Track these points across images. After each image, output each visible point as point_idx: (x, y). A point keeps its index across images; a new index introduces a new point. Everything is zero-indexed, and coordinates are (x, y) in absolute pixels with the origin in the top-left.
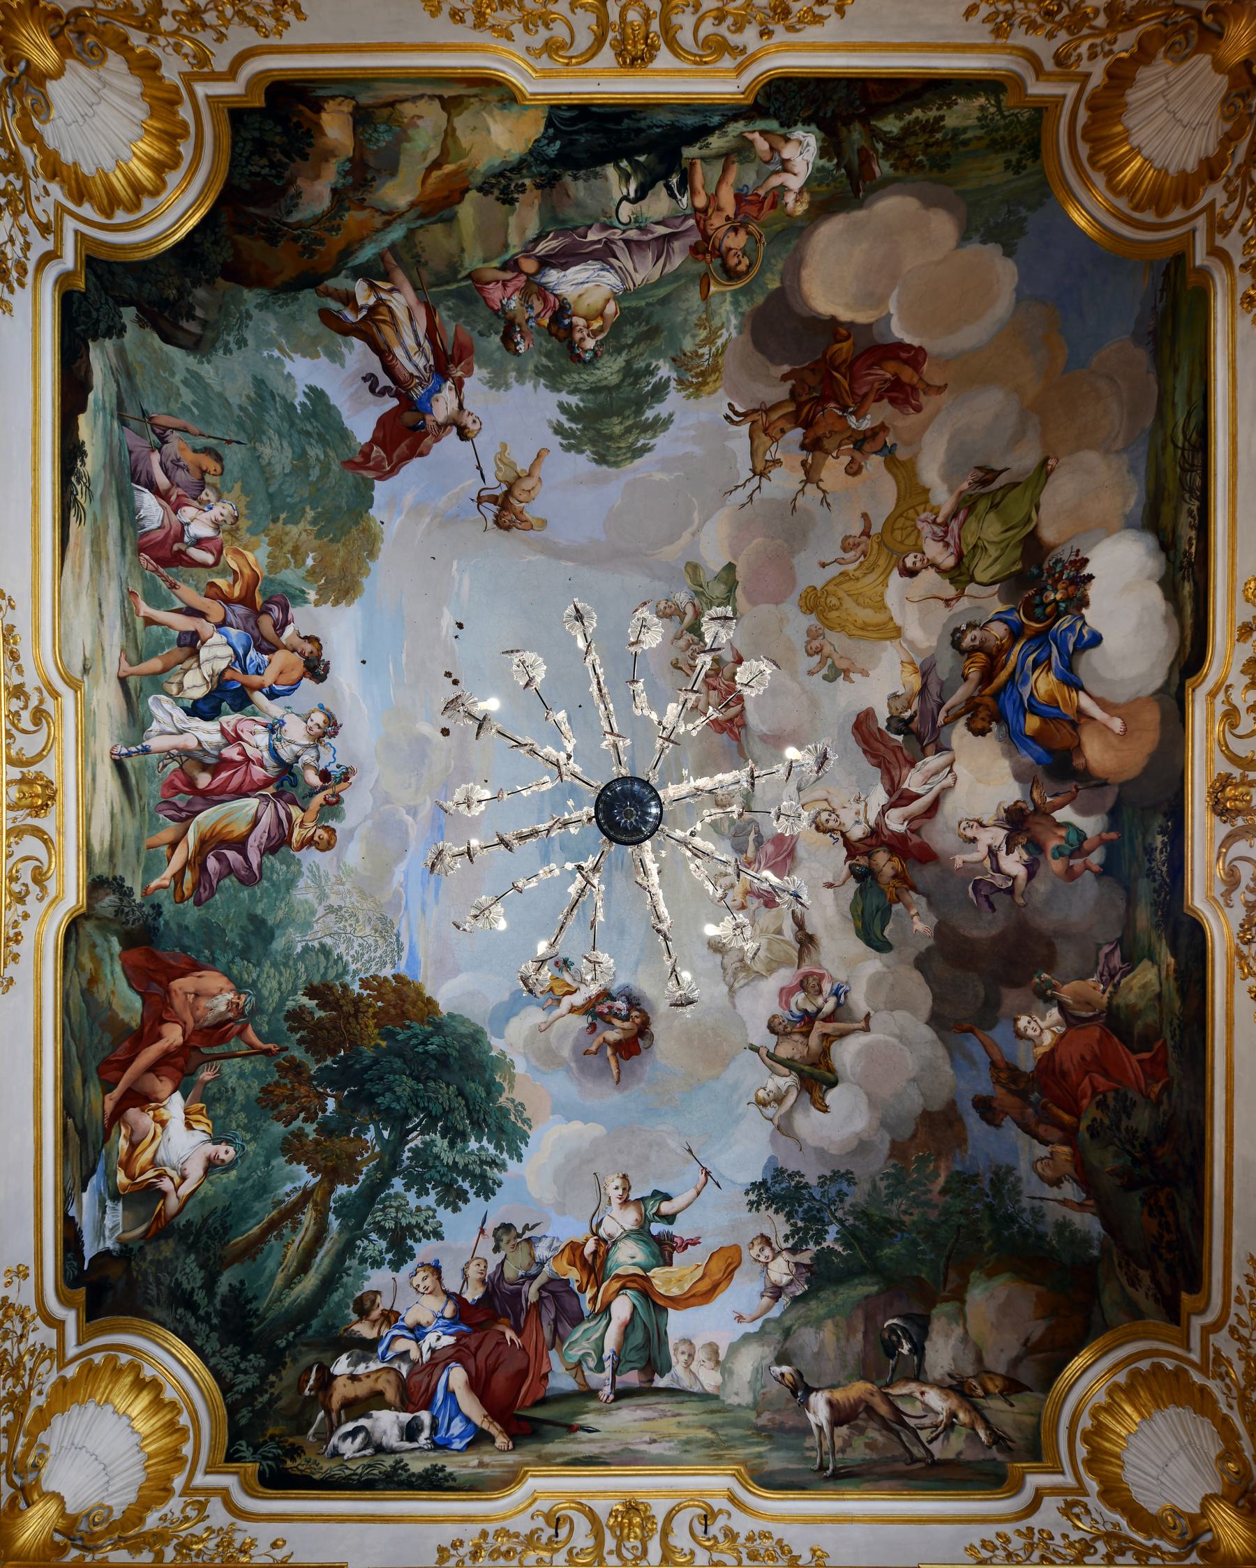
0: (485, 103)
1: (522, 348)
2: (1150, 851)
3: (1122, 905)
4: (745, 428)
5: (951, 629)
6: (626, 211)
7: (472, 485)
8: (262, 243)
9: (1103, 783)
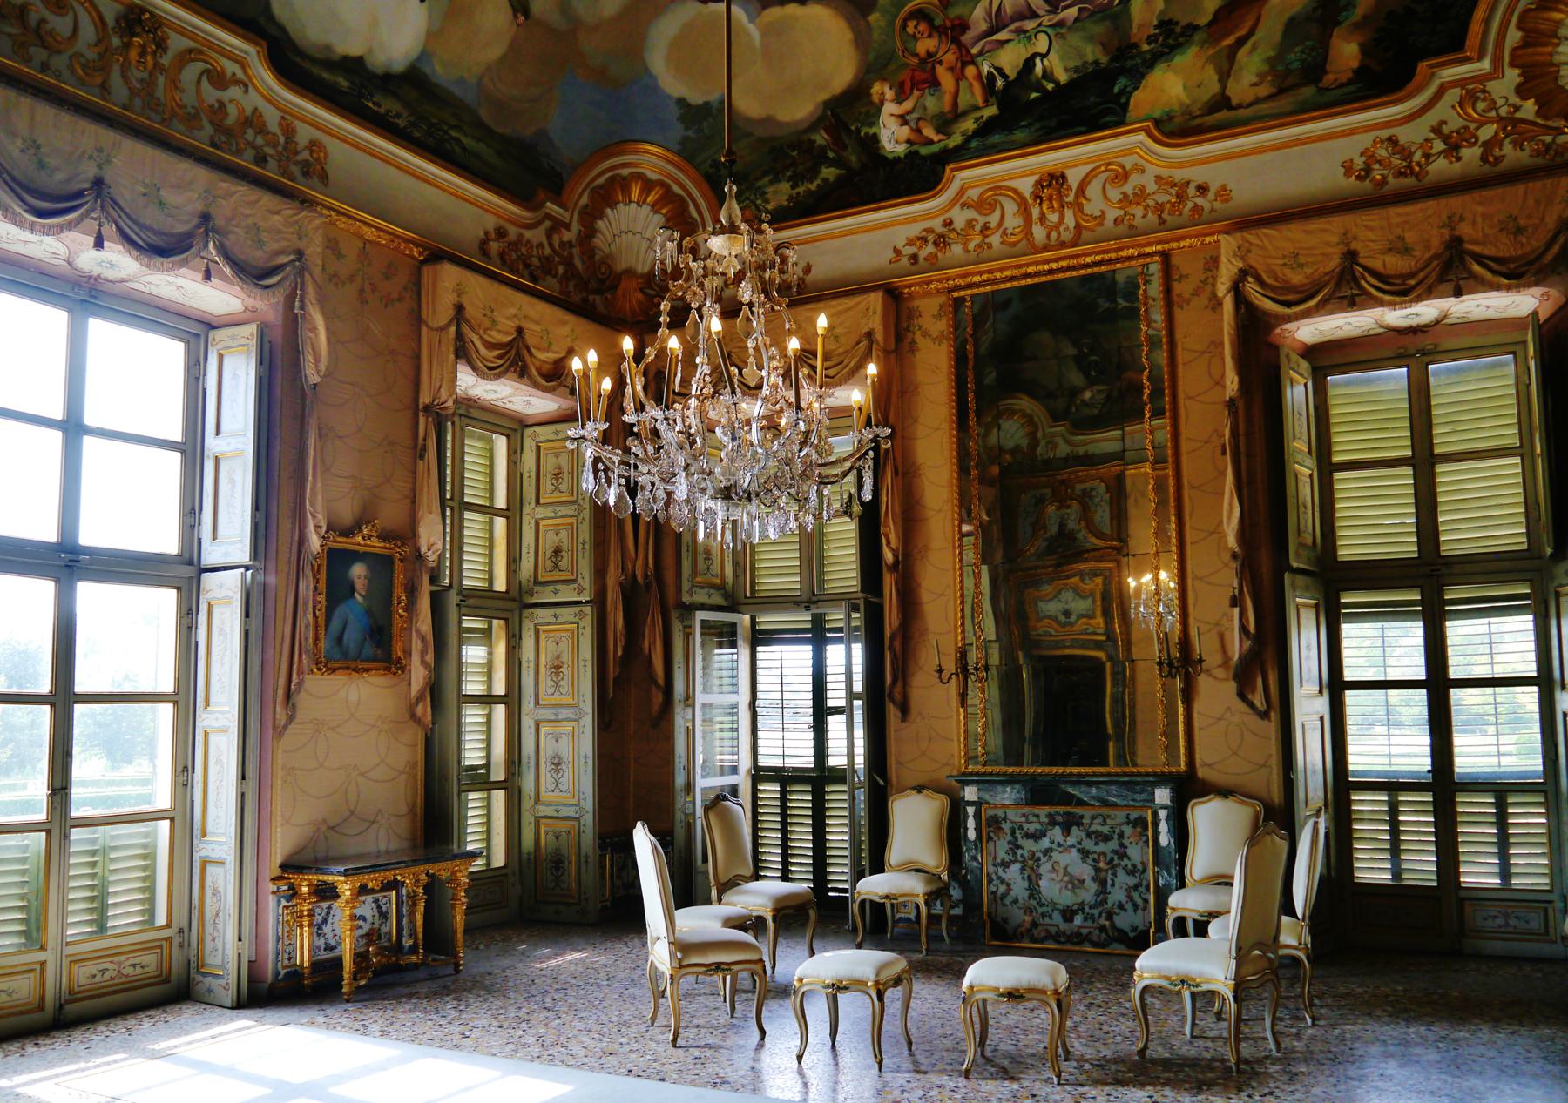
0: (1187, 112)
6: (1042, 44)
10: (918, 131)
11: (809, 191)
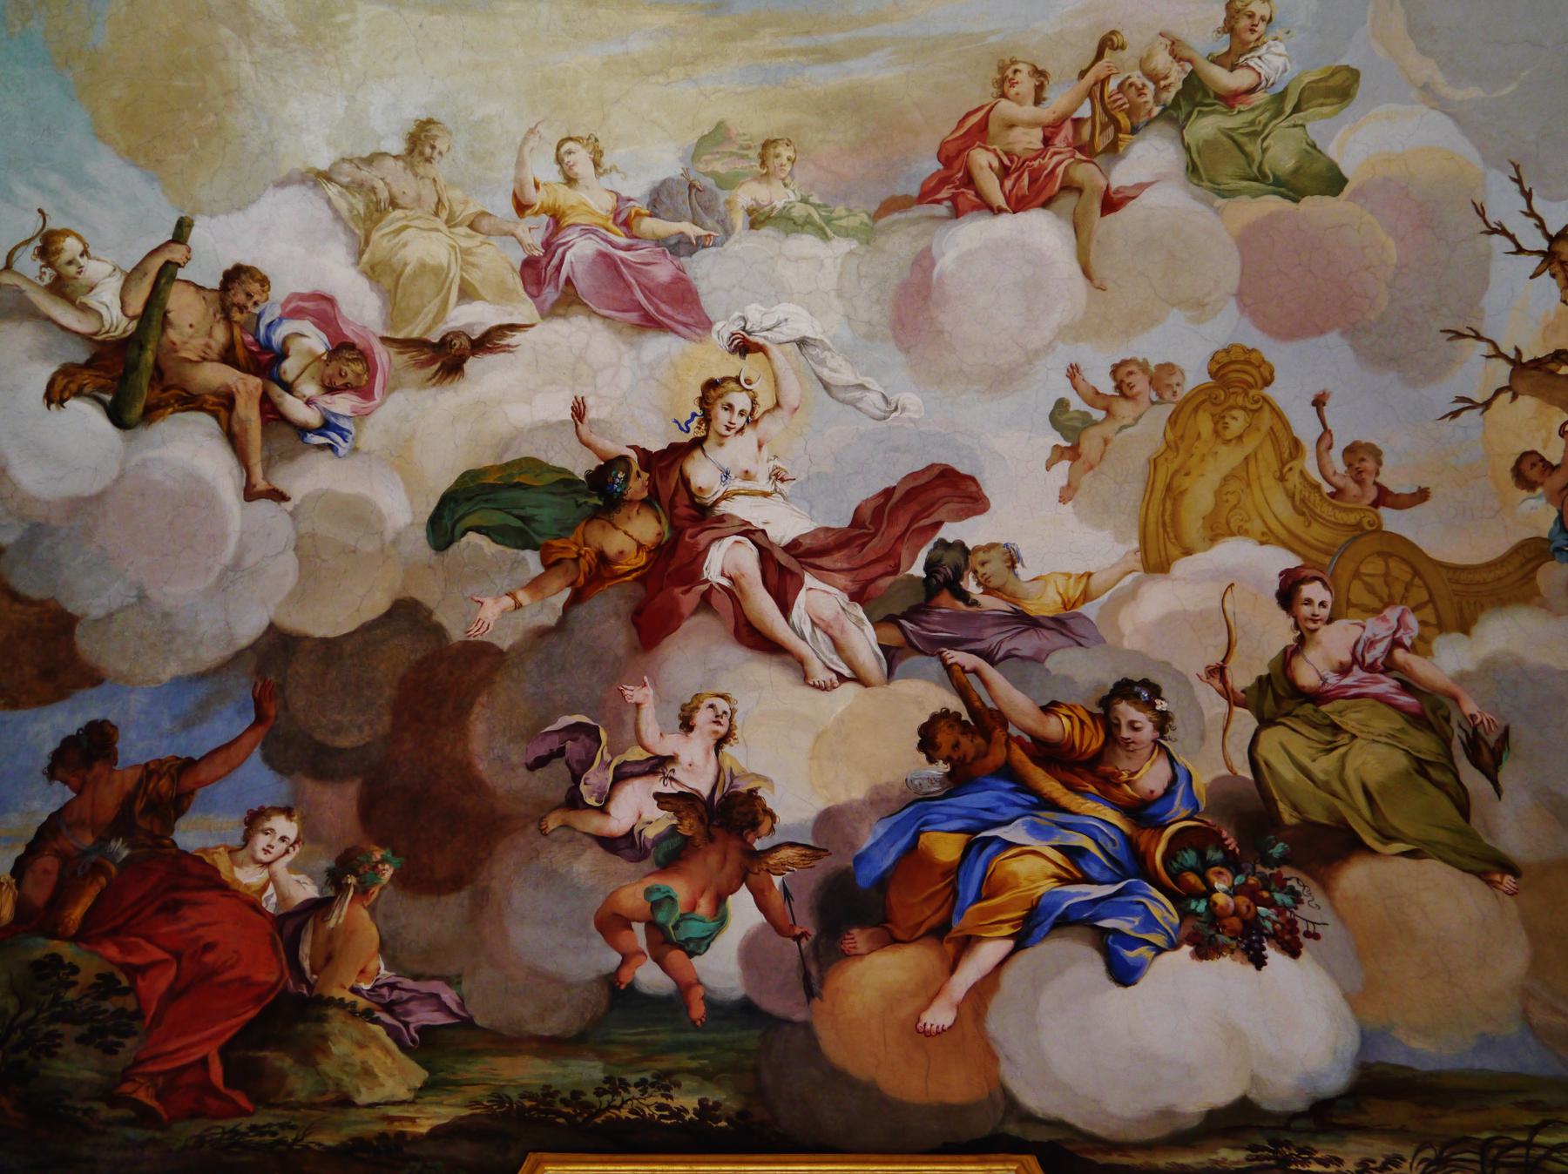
2: (665, 1082)
3: (552, 1026)
5: (1156, 678)
9: (810, 991)
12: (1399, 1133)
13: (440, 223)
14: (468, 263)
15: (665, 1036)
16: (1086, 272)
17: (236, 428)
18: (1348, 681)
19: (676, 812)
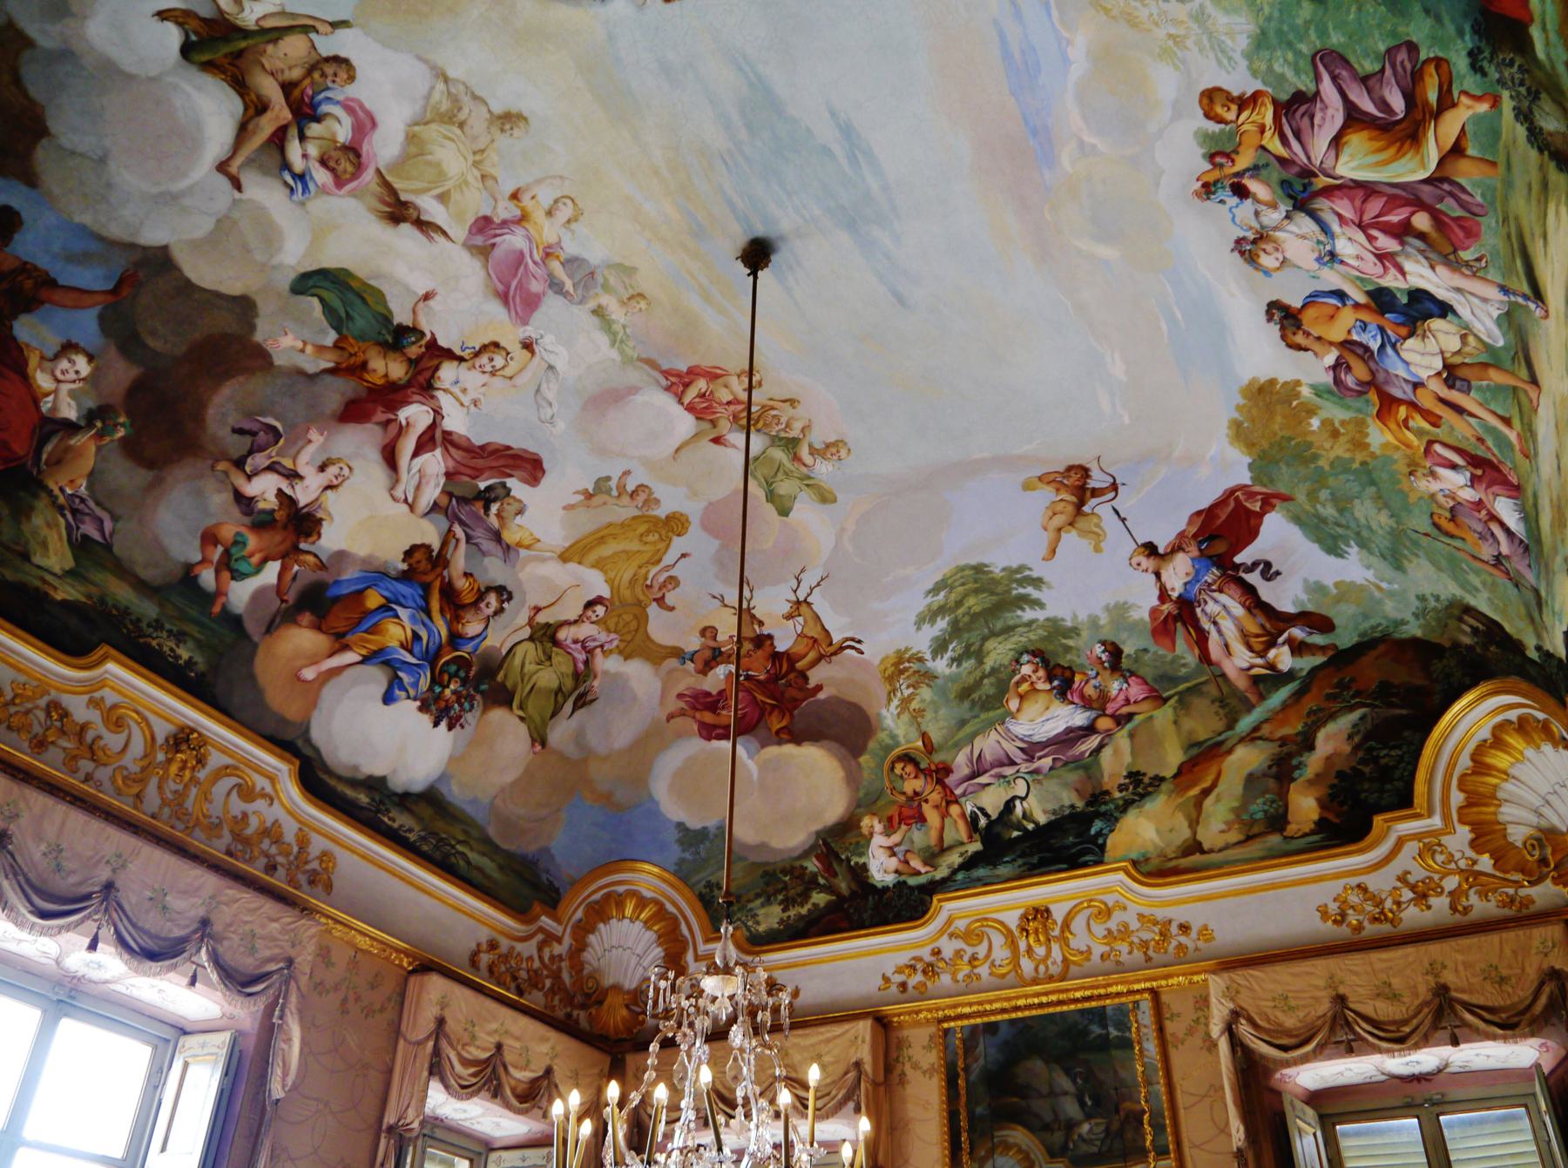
0: (1162, 855)
1: (1099, 649)
2: (180, 637)
3: (146, 574)
4: (837, 638)
7: (1124, 502)
8: (1396, 681)
9: (270, 628)
10: (907, 862)
11: (801, 917)
12: (420, 819)
13: (471, 158)
14: (460, 186)
15: (194, 613)
16: (677, 450)
17: (251, 126)
18: (573, 646)
19: (281, 504)
